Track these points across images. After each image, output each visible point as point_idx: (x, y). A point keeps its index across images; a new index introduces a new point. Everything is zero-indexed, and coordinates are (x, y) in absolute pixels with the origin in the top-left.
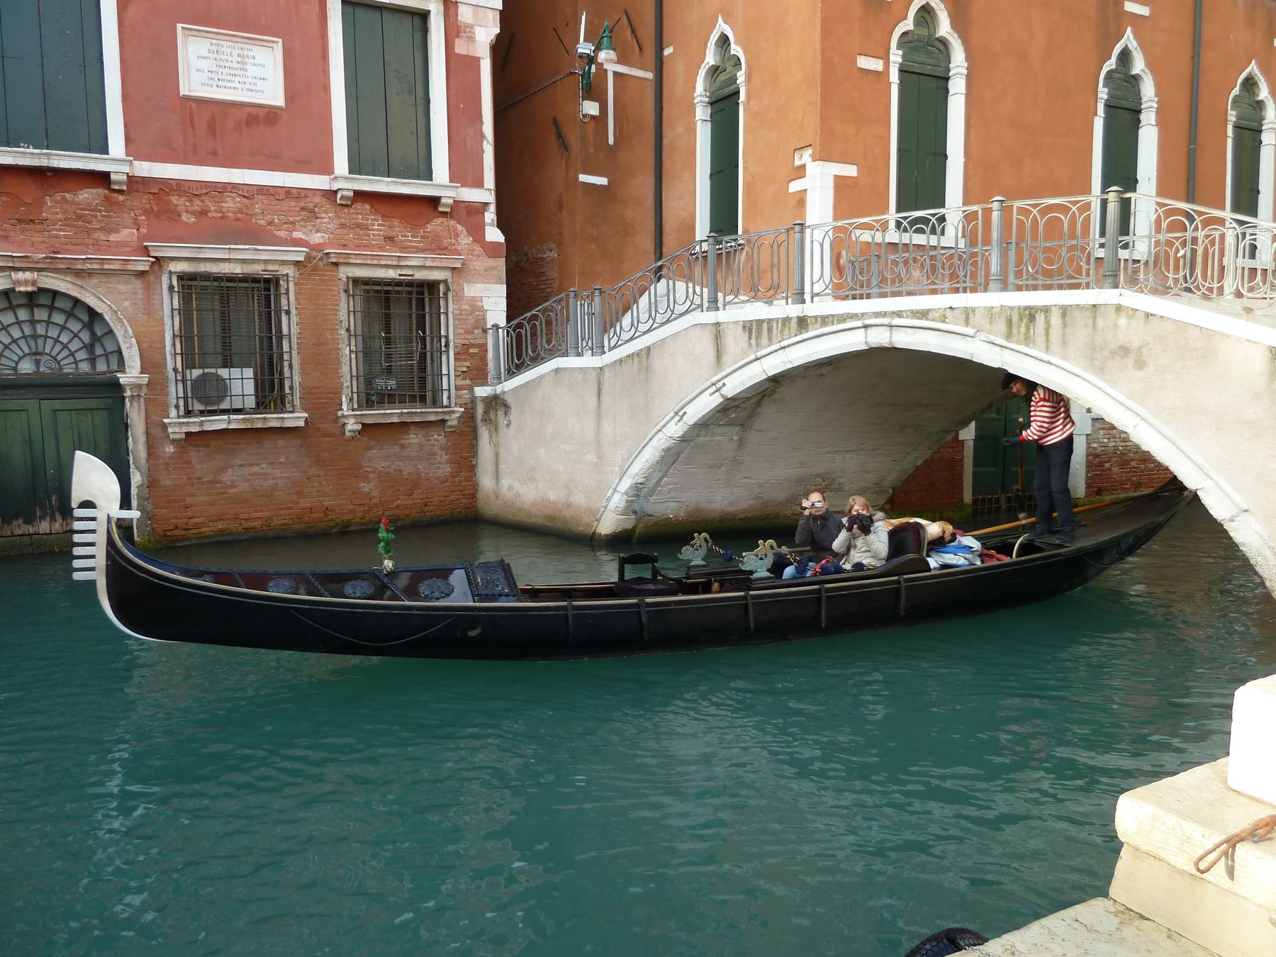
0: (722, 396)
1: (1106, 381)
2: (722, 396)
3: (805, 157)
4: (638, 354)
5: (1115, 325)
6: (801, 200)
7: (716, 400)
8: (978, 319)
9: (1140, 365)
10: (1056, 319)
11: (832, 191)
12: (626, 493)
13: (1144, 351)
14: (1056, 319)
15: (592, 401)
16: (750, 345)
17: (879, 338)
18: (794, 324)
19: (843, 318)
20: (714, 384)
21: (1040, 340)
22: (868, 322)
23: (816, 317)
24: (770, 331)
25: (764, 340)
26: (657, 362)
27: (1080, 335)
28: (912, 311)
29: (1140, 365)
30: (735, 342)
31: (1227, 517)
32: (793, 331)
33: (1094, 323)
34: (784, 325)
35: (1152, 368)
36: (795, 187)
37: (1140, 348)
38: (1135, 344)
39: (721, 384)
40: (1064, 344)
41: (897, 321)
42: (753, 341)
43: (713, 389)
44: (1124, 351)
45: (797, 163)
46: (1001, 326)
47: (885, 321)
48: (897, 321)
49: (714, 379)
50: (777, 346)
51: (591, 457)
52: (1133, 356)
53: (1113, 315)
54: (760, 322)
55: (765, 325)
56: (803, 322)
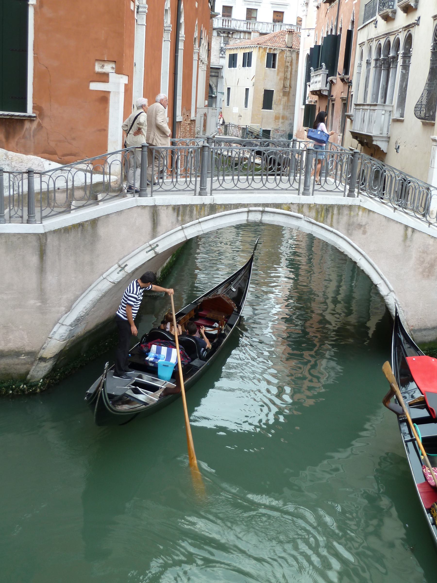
0: (155, 252)
1: (352, 240)
2: (155, 252)
3: (108, 68)
4: (81, 225)
5: (358, 214)
6: (104, 98)
7: (151, 254)
8: (305, 210)
9: (364, 233)
10: (335, 211)
11: (124, 94)
12: (70, 325)
13: (367, 227)
14: (335, 211)
15: (34, 260)
16: (178, 220)
17: (255, 217)
18: (207, 210)
19: (237, 206)
20: (150, 246)
21: (329, 221)
22: (251, 209)
23: (221, 205)
24: (191, 211)
25: (187, 218)
26: (102, 230)
27: (344, 219)
28: (273, 204)
29: (364, 233)
30: (167, 218)
31: (386, 294)
32: (206, 213)
33: (350, 214)
34: (201, 209)
35: (369, 234)
36: (94, 86)
37: (365, 225)
38: (364, 223)
39: (155, 245)
40: (338, 222)
41: (267, 209)
42: (180, 218)
43: (150, 248)
44: (360, 226)
45: (98, 68)
46: (313, 214)
47: (261, 209)
48: (267, 209)
49: (151, 242)
50: (197, 221)
51: (33, 302)
52: (362, 229)
53: (357, 209)
54: (185, 206)
55: (188, 208)
56: (213, 208)
